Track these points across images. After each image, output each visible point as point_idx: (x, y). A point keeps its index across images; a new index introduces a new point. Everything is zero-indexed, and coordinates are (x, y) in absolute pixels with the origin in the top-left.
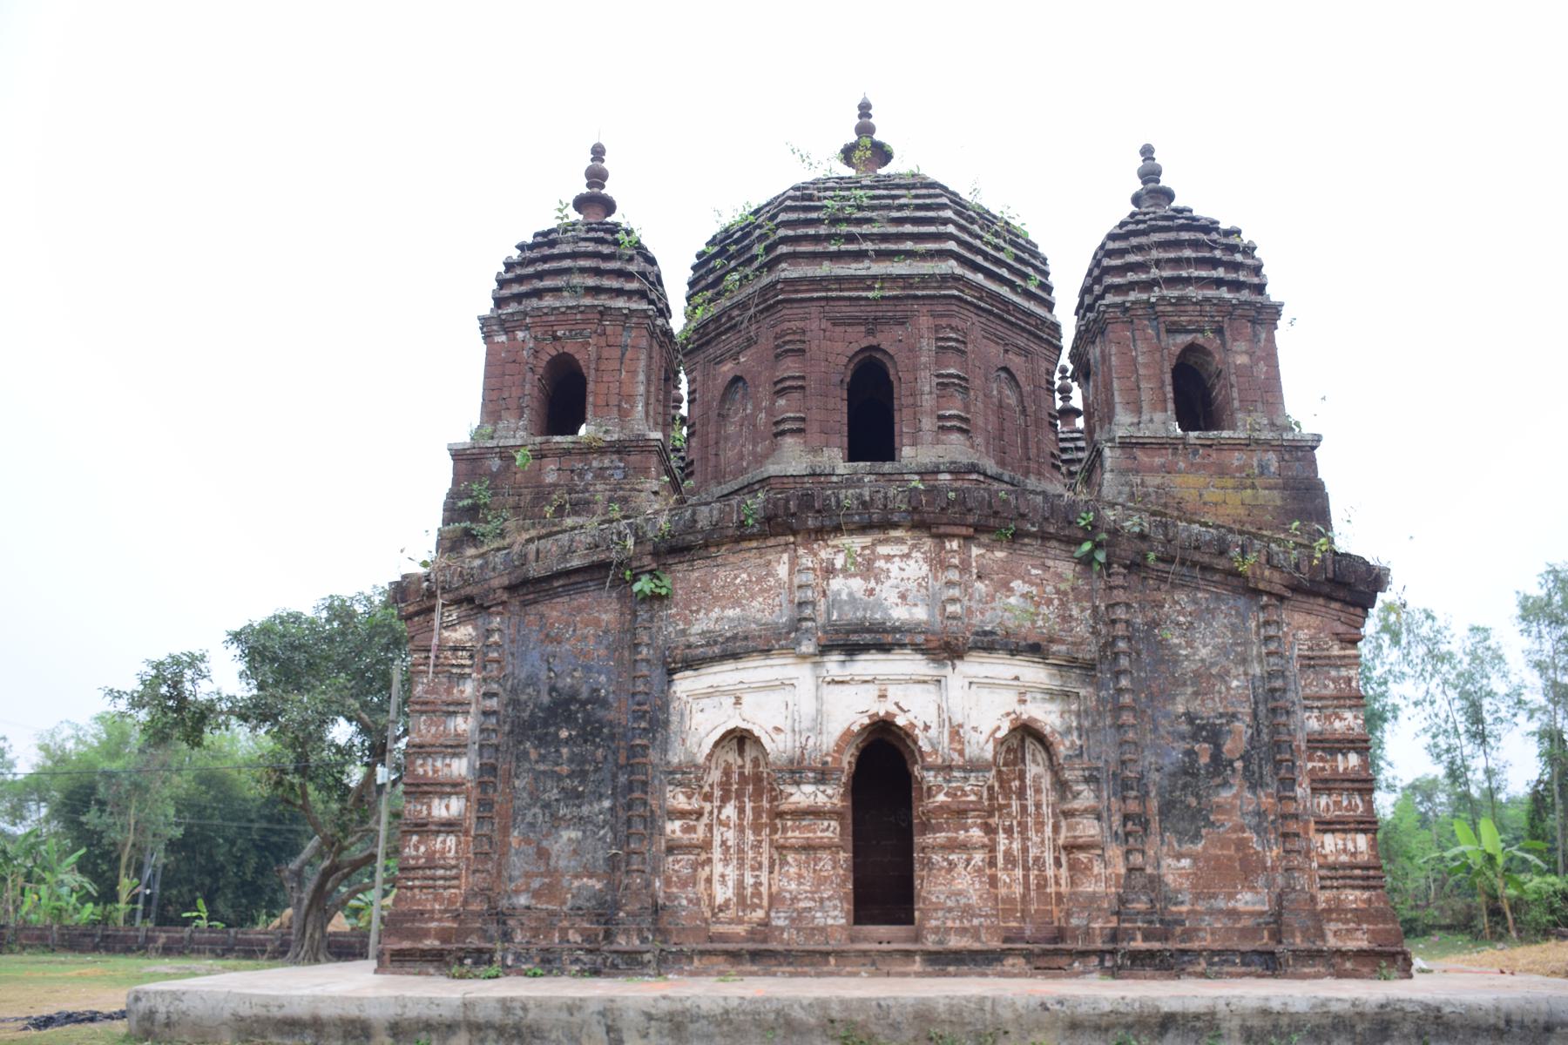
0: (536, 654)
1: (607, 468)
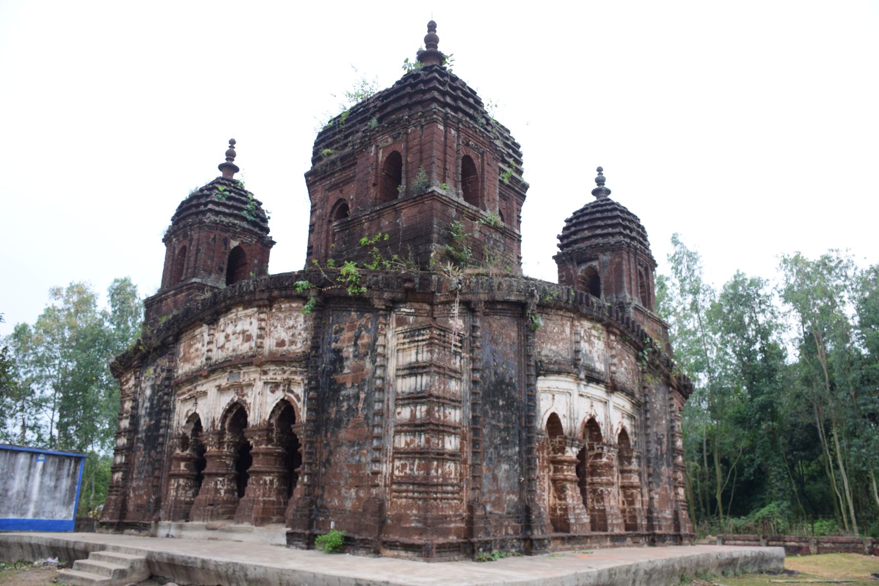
0: (487, 350)
1: (498, 241)
